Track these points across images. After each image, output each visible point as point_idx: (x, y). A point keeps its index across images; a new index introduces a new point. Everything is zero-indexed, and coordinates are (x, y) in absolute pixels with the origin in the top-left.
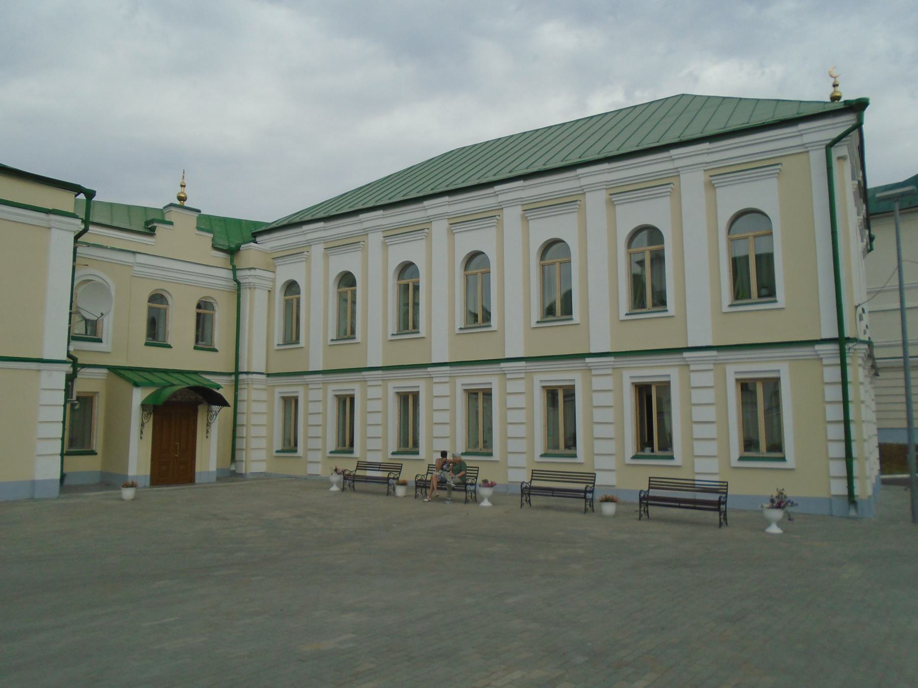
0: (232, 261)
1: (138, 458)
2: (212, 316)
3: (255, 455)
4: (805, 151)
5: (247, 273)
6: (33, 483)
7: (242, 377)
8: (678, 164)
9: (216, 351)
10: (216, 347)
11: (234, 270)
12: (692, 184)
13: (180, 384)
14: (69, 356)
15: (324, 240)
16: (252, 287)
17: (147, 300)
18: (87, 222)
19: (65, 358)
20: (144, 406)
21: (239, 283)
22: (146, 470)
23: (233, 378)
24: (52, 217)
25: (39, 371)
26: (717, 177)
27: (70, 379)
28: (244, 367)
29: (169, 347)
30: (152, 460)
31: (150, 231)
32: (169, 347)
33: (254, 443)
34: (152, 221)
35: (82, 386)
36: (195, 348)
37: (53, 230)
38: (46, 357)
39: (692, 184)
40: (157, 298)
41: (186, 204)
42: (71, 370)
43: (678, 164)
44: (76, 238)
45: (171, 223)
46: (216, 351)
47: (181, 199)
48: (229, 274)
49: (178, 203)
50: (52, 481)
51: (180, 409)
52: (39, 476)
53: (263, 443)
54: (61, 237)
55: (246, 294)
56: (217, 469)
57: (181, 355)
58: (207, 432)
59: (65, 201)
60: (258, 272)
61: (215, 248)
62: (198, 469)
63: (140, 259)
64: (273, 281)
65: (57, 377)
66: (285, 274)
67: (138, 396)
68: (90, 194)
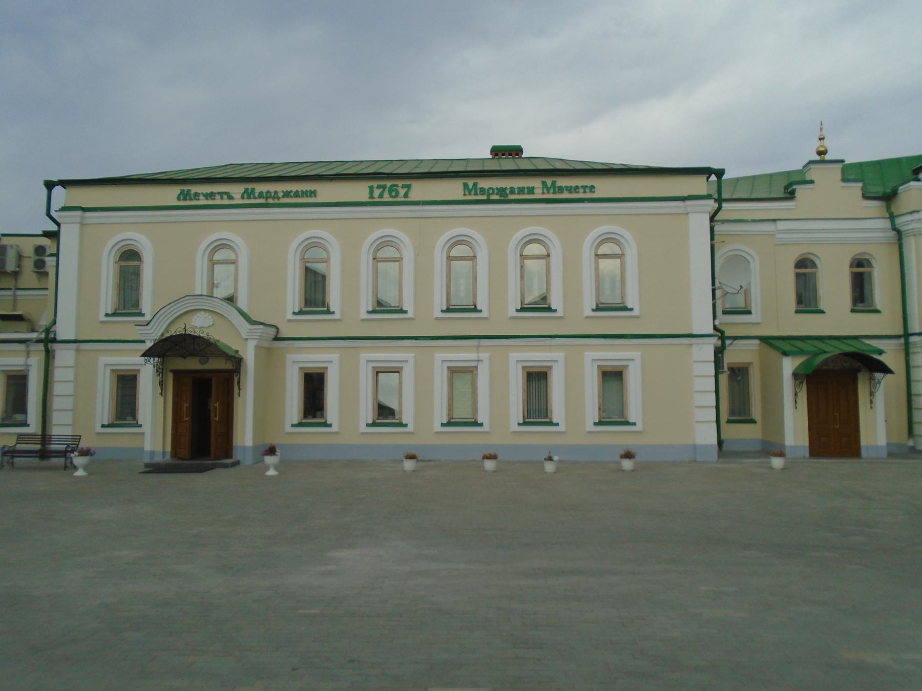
0: (888, 208)
1: (795, 428)
2: (870, 274)
6: (695, 447)
9: (878, 311)
10: (879, 307)
11: (892, 217)
13: (833, 350)
14: (715, 328)
17: (792, 265)
18: (720, 201)
19: (711, 331)
20: (796, 375)
21: (899, 232)
22: (803, 440)
23: (902, 341)
24: (688, 203)
25: (691, 345)
27: (719, 352)
29: (822, 312)
30: (809, 431)
31: (790, 195)
32: (822, 312)
34: (791, 184)
35: (732, 357)
36: (852, 311)
37: (690, 215)
38: (695, 333)
40: (804, 264)
41: (827, 157)
42: (720, 342)
44: (712, 219)
45: (812, 182)
46: (878, 311)
47: (820, 153)
48: (886, 224)
49: (818, 158)
50: (712, 446)
51: (837, 379)
52: (699, 441)
54: (698, 220)
56: (888, 444)
57: (837, 318)
58: (871, 402)
59: (699, 185)
61: (866, 197)
62: (864, 441)
63: (781, 225)
65: (706, 350)
67: (789, 365)
68: (720, 173)
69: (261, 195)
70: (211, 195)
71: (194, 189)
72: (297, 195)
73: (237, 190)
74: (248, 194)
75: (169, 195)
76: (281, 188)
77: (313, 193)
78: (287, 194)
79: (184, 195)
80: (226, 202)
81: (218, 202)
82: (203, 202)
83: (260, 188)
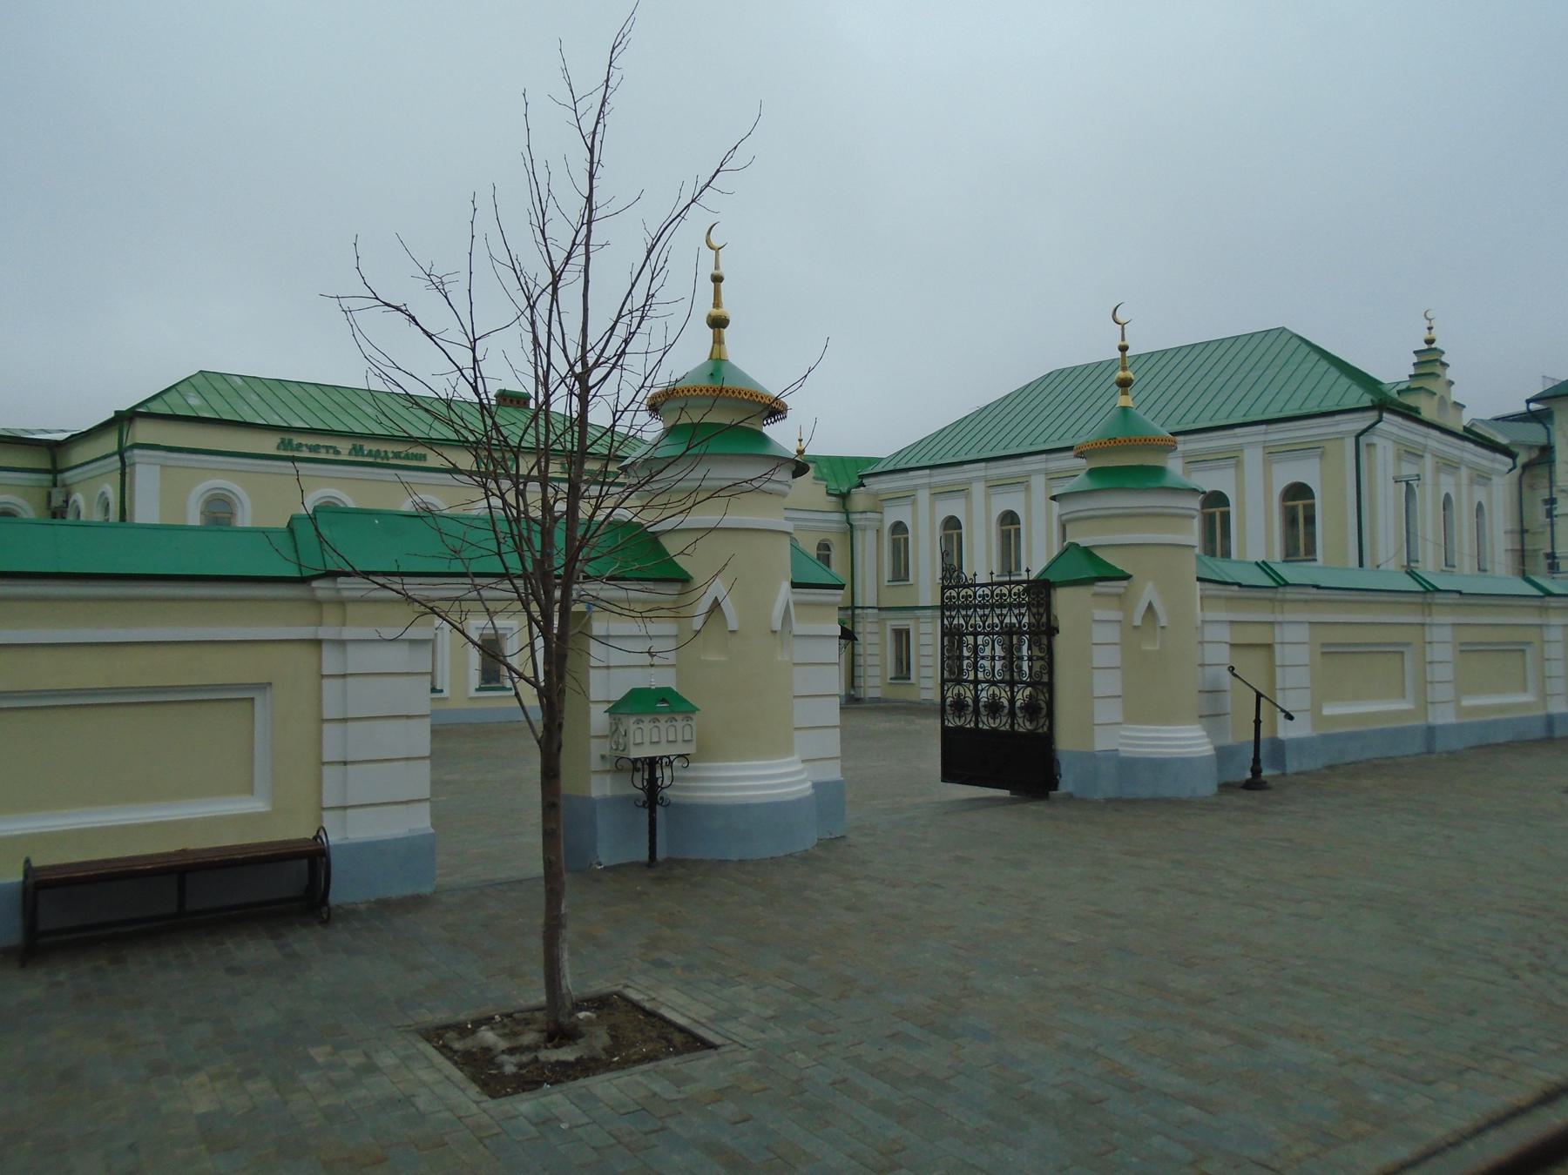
3: (871, 682)
4: (1341, 438)
5: (858, 516)
7: (858, 611)
8: (1241, 441)
11: (847, 513)
12: (1253, 458)
15: (930, 486)
16: (864, 529)
26: (1273, 453)
28: (859, 603)
33: (871, 671)
39: (1253, 458)
43: (1241, 441)
53: (877, 671)
55: (858, 535)
60: (869, 515)
61: (829, 494)
64: (881, 521)
66: (892, 515)
69: (370, 454)
70: (315, 448)
71: (297, 440)
72: (407, 457)
73: (344, 447)
74: (356, 450)
75: (269, 444)
76: (391, 448)
77: (424, 457)
78: (397, 455)
79: (284, 445)
80: (331, 456)
81: (323, 455)
82: (306, 454)
83: (369, 446)
